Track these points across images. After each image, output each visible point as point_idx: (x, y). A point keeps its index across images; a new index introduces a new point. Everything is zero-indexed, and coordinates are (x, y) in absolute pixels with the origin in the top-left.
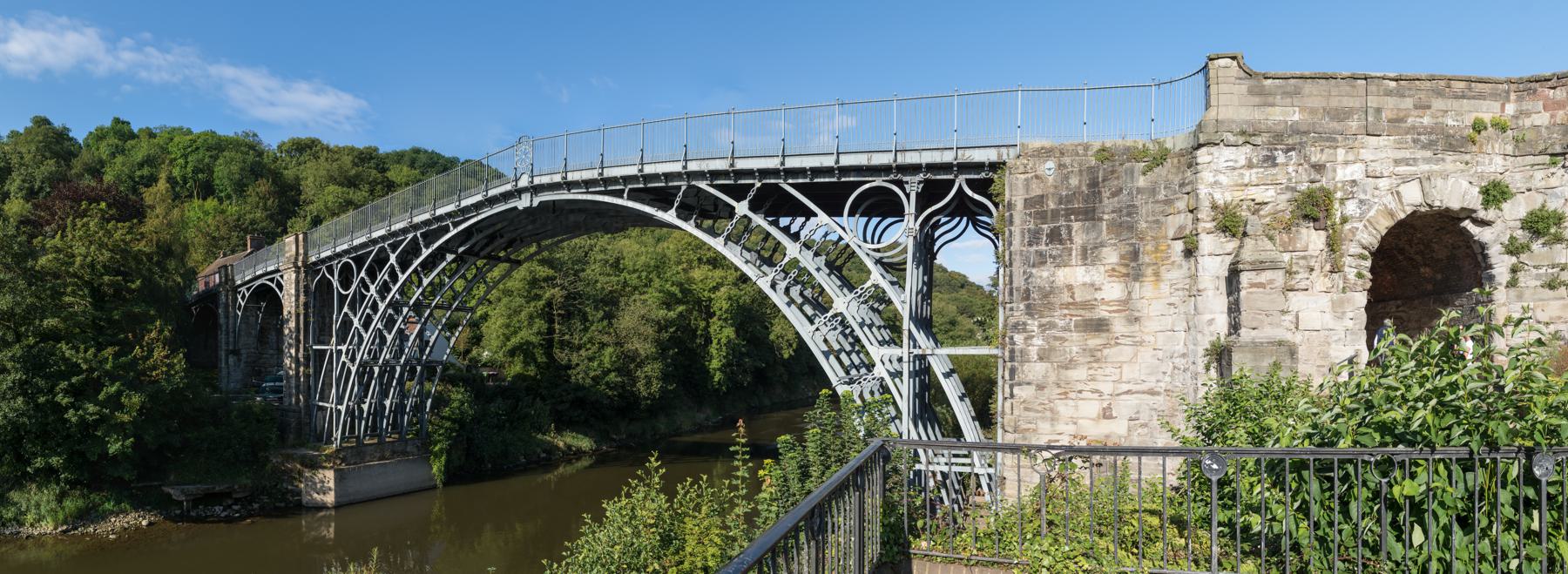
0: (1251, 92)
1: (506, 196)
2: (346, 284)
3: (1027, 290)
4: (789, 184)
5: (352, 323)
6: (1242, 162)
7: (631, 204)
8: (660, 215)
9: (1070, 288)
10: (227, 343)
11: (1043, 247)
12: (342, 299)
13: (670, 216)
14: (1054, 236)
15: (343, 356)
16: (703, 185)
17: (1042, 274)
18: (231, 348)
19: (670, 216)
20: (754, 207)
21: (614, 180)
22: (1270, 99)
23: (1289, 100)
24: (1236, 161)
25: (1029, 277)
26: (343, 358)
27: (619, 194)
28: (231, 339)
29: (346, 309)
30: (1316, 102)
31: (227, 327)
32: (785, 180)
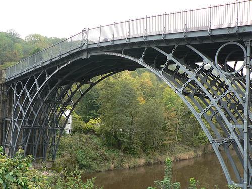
2: (18, 93)
4: (190, 45)
7: (125, 57)
8: (136, 61)
12: (17, 97)
13: (140, 61)
16: (154, 47)
19: (140, 61)
20: (174, 56)
21: (117, 46)
26: (16, 124)
27: (120, 52)
29: (18, 103)
32: (188, 43)
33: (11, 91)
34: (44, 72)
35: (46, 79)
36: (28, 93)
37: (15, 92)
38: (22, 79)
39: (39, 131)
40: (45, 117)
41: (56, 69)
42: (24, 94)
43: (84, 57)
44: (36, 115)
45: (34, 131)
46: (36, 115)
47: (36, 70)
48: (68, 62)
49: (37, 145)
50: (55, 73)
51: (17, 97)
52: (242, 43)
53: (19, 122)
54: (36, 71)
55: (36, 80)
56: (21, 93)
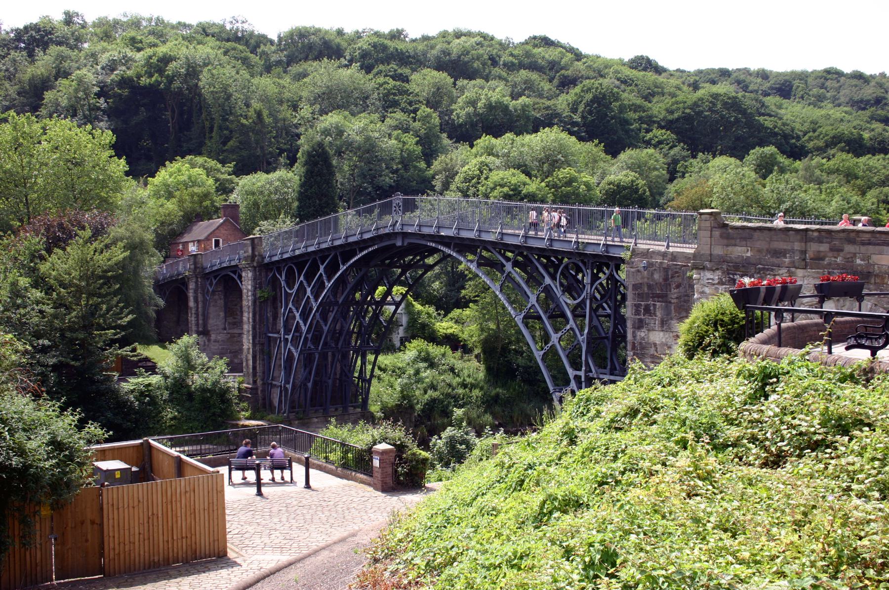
0: (721, 236)
1: (388, 236)
3: (634, 343)
5: (294, 317)
6: (716, 282)
9: (655, 345)
10: (197, 325)
11: (642, 317)
14: (647, 310)
15: (289, 344)
17: (641, 334)
18: (201, 329)
22: (733, 242)
23: (744, 243)
24: (712, 279)
25: (634, 337)
28: (201, 322)
29: (290, 305)
30: (759, 244)
31: (197, 310)
33: (275, 282)
34: (335, 257)
35: (338, 269)
36: (309, 290)
37: (283, 283)
38: (295, 261)
39: (334, 355)
40: (342, 327)
41: (356, 255)
42: (302, 290)
43: (399, 243)
44: (326, 329)
45: (324, 356)
46: (326, 329)
47: (322, 251)
48: (374, 245)
49: (330, 382)
50: (353, 260)
51: (288, 295)
52: (584, 263)
53: (295, 341)
54: (322, 254)
55: (322, 268)
56: (296, 287)
